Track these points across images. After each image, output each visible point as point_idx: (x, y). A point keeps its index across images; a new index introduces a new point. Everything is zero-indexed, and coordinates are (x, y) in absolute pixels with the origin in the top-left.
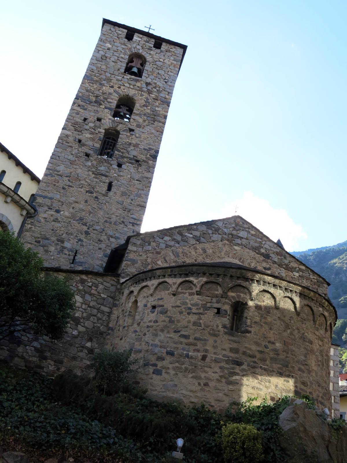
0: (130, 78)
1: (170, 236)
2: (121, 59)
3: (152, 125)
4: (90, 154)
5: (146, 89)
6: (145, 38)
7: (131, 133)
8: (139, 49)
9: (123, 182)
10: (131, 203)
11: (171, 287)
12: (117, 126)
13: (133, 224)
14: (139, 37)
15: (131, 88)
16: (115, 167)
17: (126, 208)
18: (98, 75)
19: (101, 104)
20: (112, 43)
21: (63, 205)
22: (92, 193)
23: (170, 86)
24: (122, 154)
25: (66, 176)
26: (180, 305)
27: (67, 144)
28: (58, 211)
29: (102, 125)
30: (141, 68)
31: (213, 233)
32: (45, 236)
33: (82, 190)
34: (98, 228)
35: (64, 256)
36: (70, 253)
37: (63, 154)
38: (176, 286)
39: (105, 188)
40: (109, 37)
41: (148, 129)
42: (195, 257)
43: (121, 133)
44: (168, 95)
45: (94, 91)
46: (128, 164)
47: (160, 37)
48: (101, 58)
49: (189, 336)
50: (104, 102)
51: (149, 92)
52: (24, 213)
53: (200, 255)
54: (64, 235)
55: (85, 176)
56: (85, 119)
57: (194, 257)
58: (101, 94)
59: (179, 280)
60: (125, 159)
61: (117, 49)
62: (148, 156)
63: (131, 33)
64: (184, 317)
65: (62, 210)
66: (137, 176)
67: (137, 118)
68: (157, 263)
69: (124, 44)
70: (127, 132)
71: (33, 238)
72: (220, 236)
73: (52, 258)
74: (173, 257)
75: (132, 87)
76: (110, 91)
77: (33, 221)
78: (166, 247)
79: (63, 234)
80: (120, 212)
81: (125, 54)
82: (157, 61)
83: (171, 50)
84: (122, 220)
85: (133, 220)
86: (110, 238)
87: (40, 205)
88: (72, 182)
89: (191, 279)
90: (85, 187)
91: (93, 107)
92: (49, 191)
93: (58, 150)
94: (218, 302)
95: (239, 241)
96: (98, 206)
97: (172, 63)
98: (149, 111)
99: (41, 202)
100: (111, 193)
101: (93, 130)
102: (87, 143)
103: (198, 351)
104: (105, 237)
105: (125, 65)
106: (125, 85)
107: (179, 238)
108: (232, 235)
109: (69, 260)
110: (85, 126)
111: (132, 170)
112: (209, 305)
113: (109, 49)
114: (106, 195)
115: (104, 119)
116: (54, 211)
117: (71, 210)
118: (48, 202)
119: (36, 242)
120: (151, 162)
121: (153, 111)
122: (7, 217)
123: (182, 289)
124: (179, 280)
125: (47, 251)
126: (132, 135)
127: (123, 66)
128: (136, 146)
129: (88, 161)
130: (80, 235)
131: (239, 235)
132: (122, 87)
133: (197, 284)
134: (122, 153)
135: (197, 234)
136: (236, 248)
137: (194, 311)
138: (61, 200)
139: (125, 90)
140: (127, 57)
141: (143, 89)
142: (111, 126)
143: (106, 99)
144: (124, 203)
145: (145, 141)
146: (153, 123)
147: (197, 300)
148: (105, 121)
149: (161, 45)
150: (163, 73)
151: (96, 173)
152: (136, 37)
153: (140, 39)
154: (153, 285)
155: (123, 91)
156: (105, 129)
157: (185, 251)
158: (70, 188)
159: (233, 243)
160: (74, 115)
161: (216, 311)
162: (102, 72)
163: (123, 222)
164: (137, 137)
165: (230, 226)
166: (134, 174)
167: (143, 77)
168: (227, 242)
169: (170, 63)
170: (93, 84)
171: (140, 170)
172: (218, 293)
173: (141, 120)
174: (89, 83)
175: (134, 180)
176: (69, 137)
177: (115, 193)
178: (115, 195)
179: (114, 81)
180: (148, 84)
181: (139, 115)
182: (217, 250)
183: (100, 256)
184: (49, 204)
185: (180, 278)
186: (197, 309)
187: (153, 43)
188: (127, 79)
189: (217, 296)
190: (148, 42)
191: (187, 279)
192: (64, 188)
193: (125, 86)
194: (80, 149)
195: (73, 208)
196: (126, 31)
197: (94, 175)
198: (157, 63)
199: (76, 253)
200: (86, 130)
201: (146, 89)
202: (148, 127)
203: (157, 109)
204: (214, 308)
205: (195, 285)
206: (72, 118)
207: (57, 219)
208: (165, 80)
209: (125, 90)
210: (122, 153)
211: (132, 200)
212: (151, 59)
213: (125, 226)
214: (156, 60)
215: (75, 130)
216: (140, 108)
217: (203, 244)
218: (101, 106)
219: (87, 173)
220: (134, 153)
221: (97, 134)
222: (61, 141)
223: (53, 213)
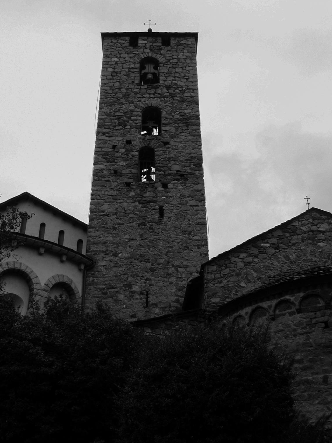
0: (148, 87)
1: (245, 252)
2: (132, 70)
3: (186, 131)
4: (130, 183)
5: (168, 94)
6: (151, 39)
7: (167, 146)
8: (148, 53)
9: (174, 203)
10: (190, 224)
11: (268, 311)
12: (149, 144)
13: (199, 247)
14: (144, 40)
15: (152, 98)
16: (161, 189)
17: (185, 231)
18: (114, 94)
19: (126, 125)
20: (118, 56)
21: (118, 246)
22: (145, 225)
23: (192, 82)
24: (164, 173)
25: (113, 215)
26: (282, 328)
27: (103, 179)
28: (115, 255)
29: (134, 148)
30: (156, 72)
31: (291, 236)
32: (111, 285)
33: (134, 224)
34: (162, 261)
35: (136, 301)
36: (141, 296)
37: (103, 192)
38: (272, 309)
39: (157, 216)
40: (113, 50)
41: (182, 136)
42: (280, 268)
43: (156, 150)
44: (193, 92)
45: (114, 113)
46: (173, 182)
47: (166, 33)
48: (112, 75)
49: (302, 359)
50: (128, 121)
51: (172, 96)
52: (82, 267)
53: (284, 264)
54: (130, 279)
55: (132, 209)
56: (114, 147)
57: (277, 268)
58: (123, 114)
59: (274, 302)
60: (169, 177)
61: (125, 61)
62: (192, 166)
63: (133, 38)
64: (291, 341)
65: (119, 252)
66: (186, 193)
67: (167, 128)
68: (240, 286)
70: (162, 147)
71: (99, 290)
72: (300, 237)
73: (124, 306)
74: (255, 275)
75: (152, 96)
76: (131, 108)
77: (93, 272)
78: (245, 265)
79: (128, 278)
80: (180, 237)
81: (135, 63)
82: (171, 59)
83: (181, 42)
84: (184, 245)
85: (197, 242)
86: (179, 269)
87: (96, 253)
88: (121, 219)
89: (287, 297)
90: (136, 221)
91: (119, 131)
92: (99, 235)
93: (97, 188)
94: (323, 316)
95: (322, 236)
96: (155, 237)
97: (186, 56)
98: (178, 117)
99: (95, 249)
100: (165, 219)
101: (125, 156)
102: (123, 172)
103: (317, 373)
104: (173, 269)
105: (138, 75)
106: (145, 96)
107: (255, 251)
108: (312, 231)
109: (143, 304)
110: (116, 154)
111: (180, 187)
112: (314, 321)
113: (116, 63)
115: (134, 141)
116: (112, 256)
117: (128, 249)
118: (102, 248)
119: (103, 293)
120: (197, 172)
121: (183, 115)
122: (67, 277)
123: (280, 311)
124: (274, 302)
125: (116, 301)
126: (169, 148)
127: (136, 76)
128: (176, 159)
129: (131, 191)
130: (146, 274)
131: (320, 229)
132: (143, 99)
133: (295, 302)
134: (164, 171)
135: (274, 241)
136: (321, 244)
137: (299, 331)
138: (115, 242)
139: (146, 102)
140: (138, 65)
141: (165, 94)
142: (144, 146)
143: (129, 118)
144: (182, 226)
145: (184, 150)
146: (186, 128)
147: (300, 319)
148: (135, 142)
149: (169, 40)
150: (180, 70)
151: (142, 202)
152: (141, 42)
153: (146, 42)
154: (246, 313)
155: (144, 104)
157: (267, 264)
158: (120, 226)
159: (316, 240)
160: (102, 145)
161: (323, 325)
162: (117, 90)
163: (187, 247)
164: (174, 149)
165: (307, 222)
166: (183, 191)
167: (161, 82)
168: (310, 242)
169: (185, 57)
170: (111, 106)
171: (188, 185)
172: (321, 305)
173: (173, 130)
174: (106, 106)
175: (185, 197)
176: (104, 171)
177: (169, 218)
178: (170, 220)
180: (168, 88)
182: (301, 254)
183: (173, 291)
184: (104, 249)
185: (275, 299)
186: (303, 328)
187: (161, 41)
188: (145, 89)
189: (320, 309)
191: (282, 298)
192: (114, 228)
193: (144, 97)
194: (118, 181)
195: (130, 247)
196: (128, 38)
197: (141, 205)
198: (171, 61)
199: (147, 295)
200: (118, 157)
201: (168, 94)
202: (182, 134)
203: (186, 111)
204: (321, 322)
205: (293, 303)
206: (100, 150)
207: (117, 263)
208: (186, 77)
209: (146, 102)
210: (164, 171)
211: (189, 220)
212: (164, 59)
213: (191, 251)
214: (169, 58)
216: (168, 117)
217: (283, 250)
218: (126, 127)
219: (133, 205)
220: (176, 167)
221: (131, 158)
222: (96, 178)
223: (112, 258)
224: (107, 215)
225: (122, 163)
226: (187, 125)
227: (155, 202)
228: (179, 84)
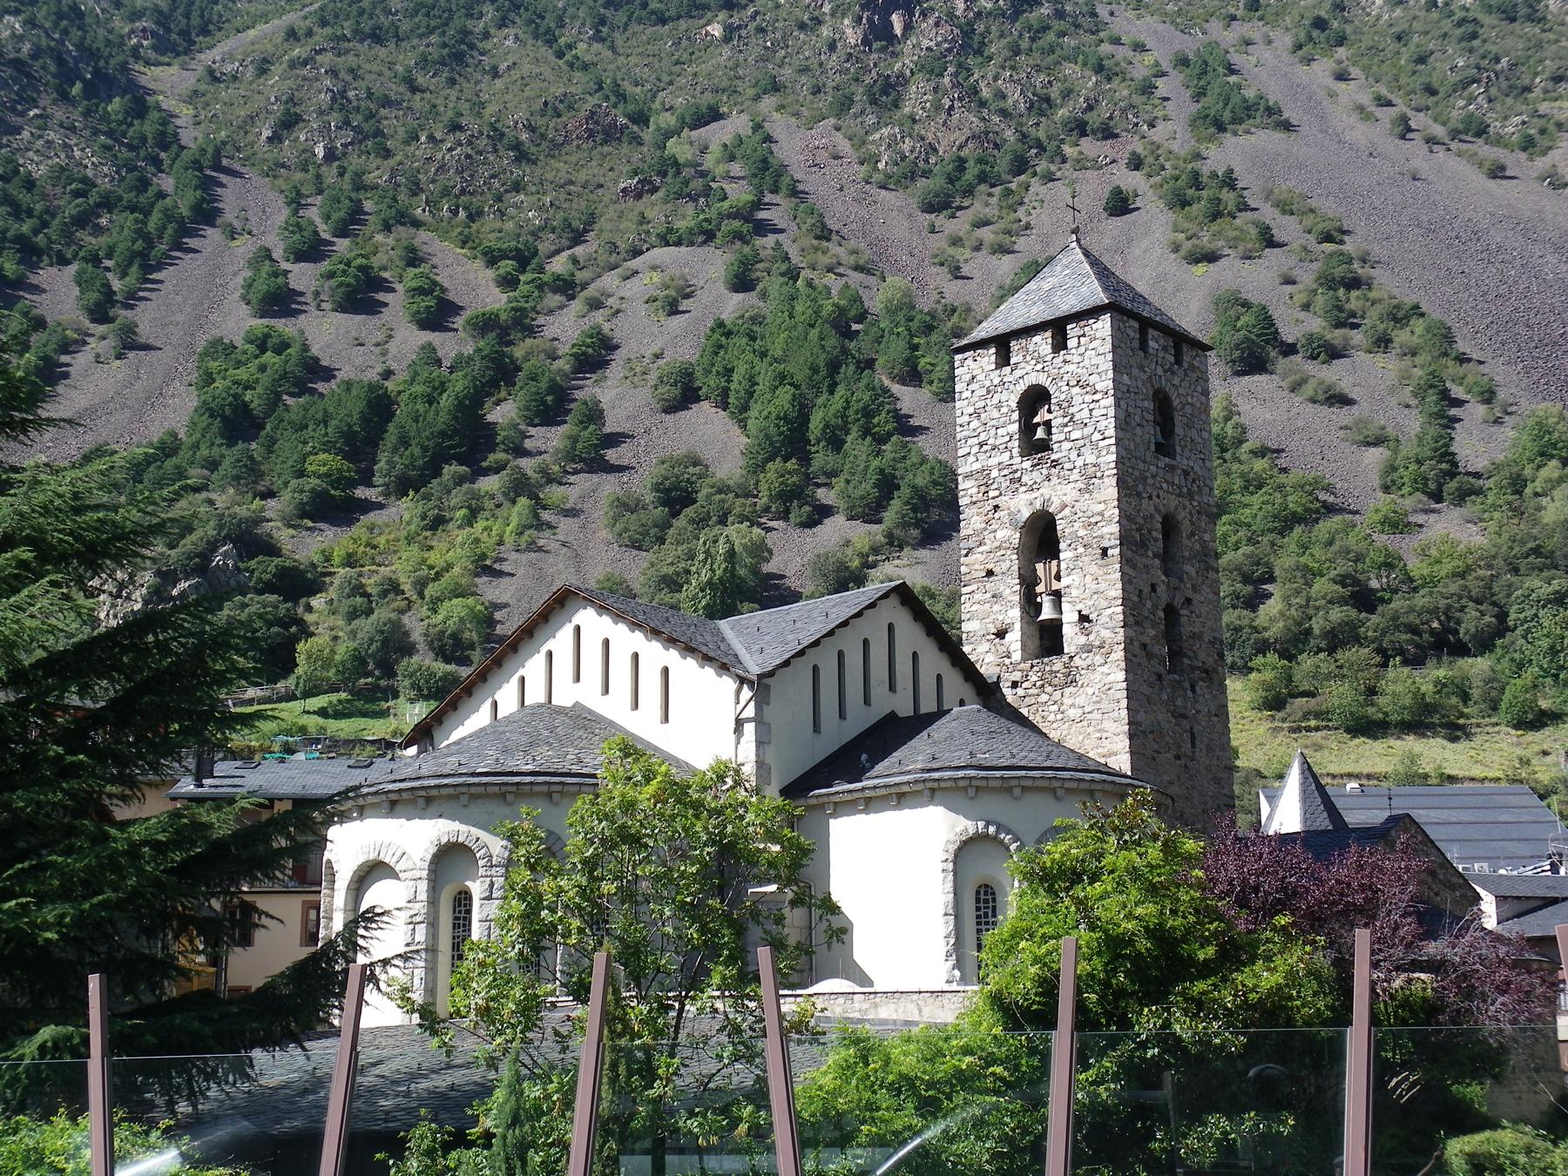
16: (1190, 693)
41: (1205, 589)
51: (1190, 495)
69: (1141, 368)
114: (1193, 759)
143: (1150, 532)
156: (1164, 610)
164: (1199, 616)
179: (1150, 481)
180: (1186, 473)
181: (1189, 559)
190: (1165, 348)
196: (1136, 325)
215: (1137, 623)
224: (1144, 732)
225: (1152, 632)
226: (1209, 568)
227: (1185, 717)
228: (1197, 468)
